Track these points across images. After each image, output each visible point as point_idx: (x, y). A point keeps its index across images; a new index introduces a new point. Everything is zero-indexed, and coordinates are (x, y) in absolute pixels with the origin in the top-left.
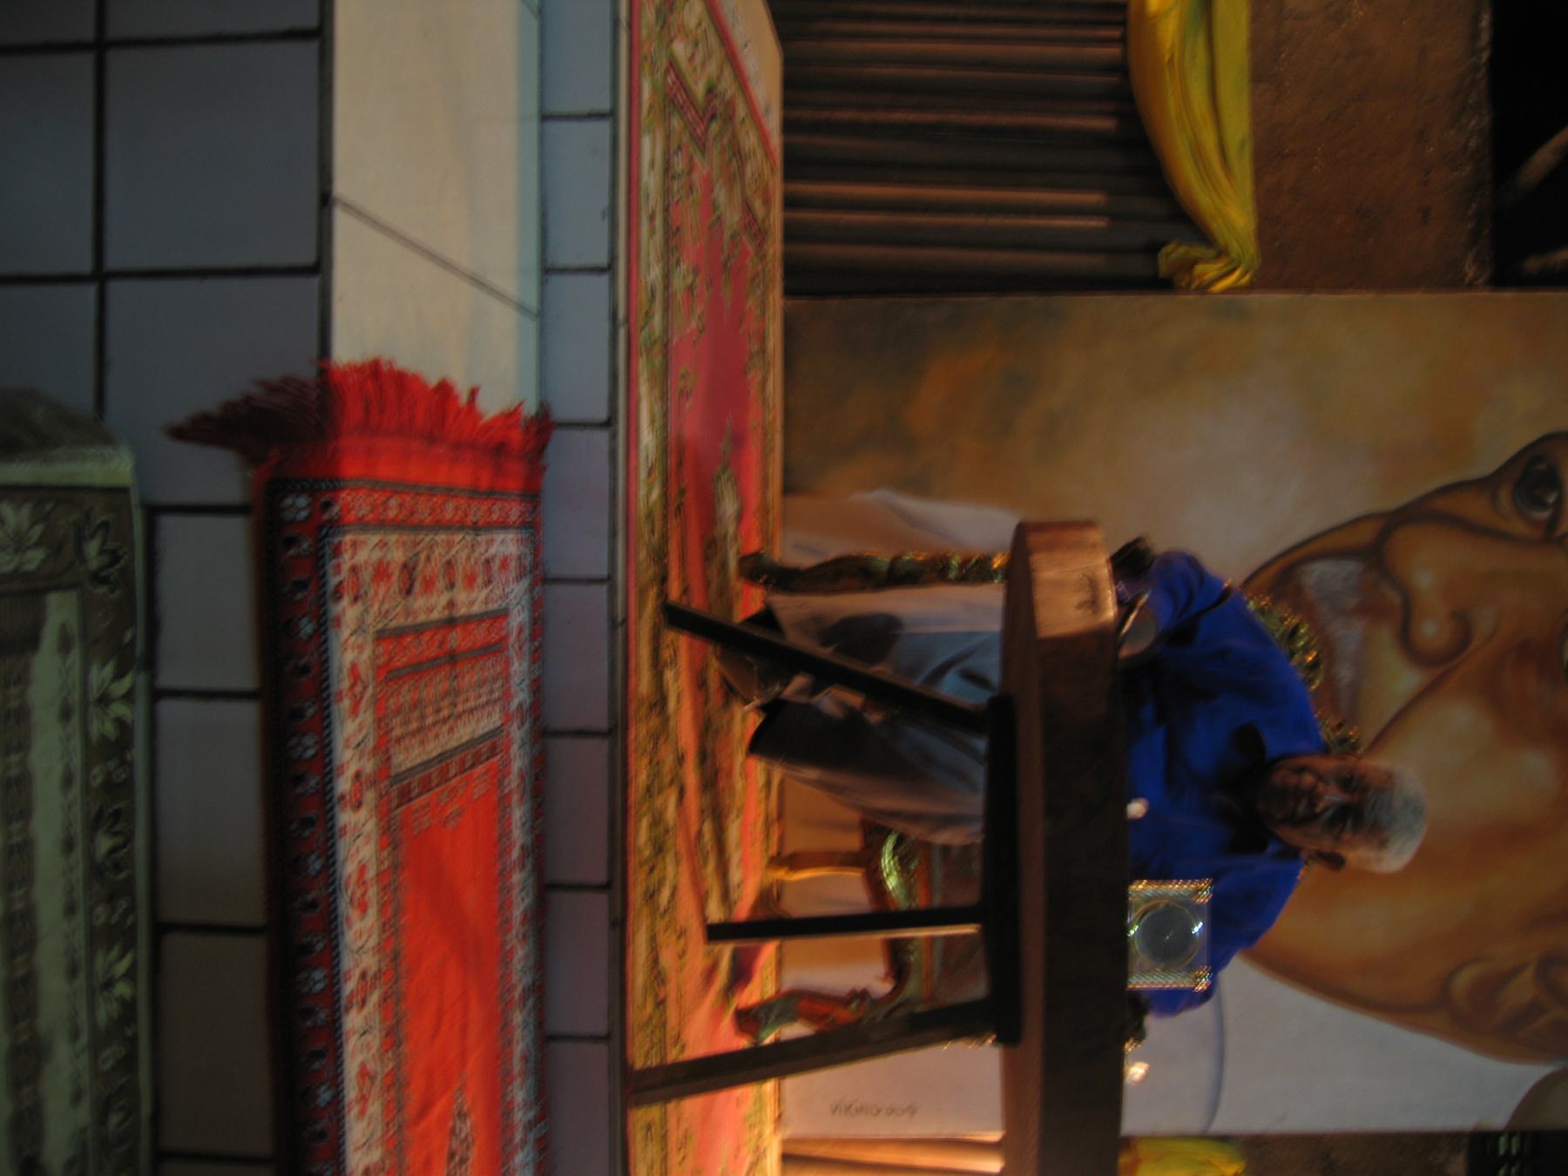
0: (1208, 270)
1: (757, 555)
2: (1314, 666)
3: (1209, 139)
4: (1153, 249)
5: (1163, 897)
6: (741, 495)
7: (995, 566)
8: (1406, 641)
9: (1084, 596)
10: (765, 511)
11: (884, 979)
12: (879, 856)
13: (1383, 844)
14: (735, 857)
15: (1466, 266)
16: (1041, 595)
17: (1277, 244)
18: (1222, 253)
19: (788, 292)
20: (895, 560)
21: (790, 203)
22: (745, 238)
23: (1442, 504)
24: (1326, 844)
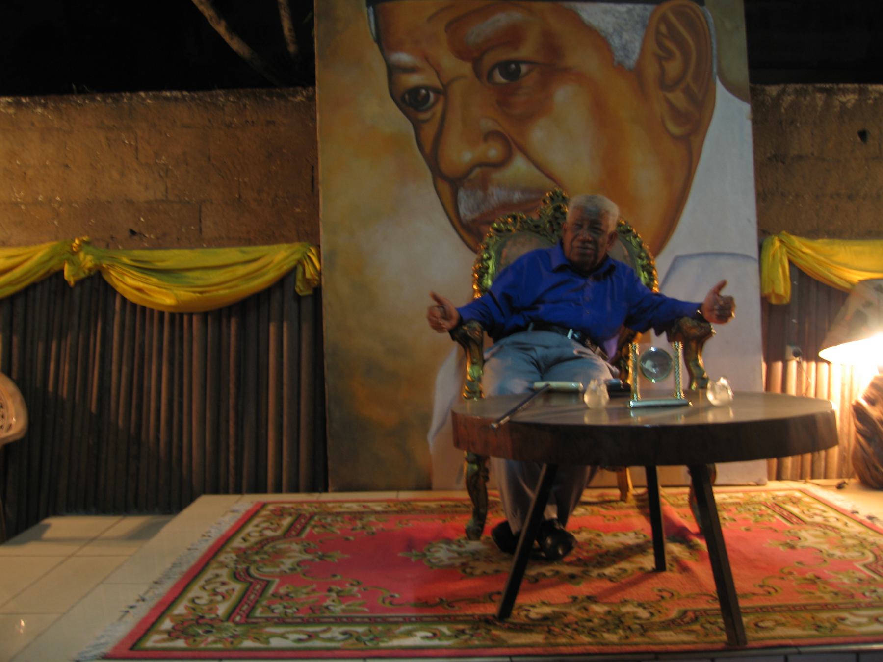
0: (310, 272)
2: (514, 218)
3: (242, 270)
4: (298, 298)
8: (500, 165)
15: (296, 100)
17: (286, 200)
18: (300, 262)
19: (326, 490)
20: (467, 459)
21: (278, 490)
22: (304, 536)
23: (428, 148)
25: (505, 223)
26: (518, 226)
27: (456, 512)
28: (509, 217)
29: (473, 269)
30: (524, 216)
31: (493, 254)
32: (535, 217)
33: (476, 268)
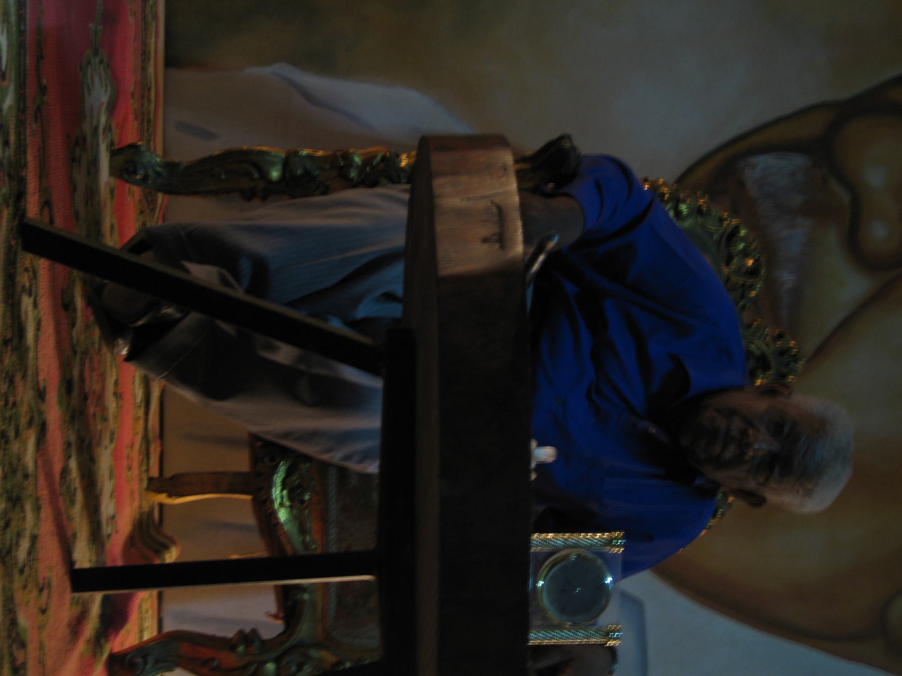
1: (133, 147)
2: (753, 272)
5: (575, 546)
6: (116, 81)
7: (403, 164)
9: (490, 229)
10: (144, 88)
11: (276, 617)
12: (270, 485)
13: (808, 493)
14: (107, 486)
16: (441, 227)
24: (751, 485)
25: (745, 253)
26: (734, 279)
27: (142, 122)
28: (757, 261)
29: (658, 179)
30: (753, 294)
31: (688, 223)
32: (746, 317)
33: (660, 186)
